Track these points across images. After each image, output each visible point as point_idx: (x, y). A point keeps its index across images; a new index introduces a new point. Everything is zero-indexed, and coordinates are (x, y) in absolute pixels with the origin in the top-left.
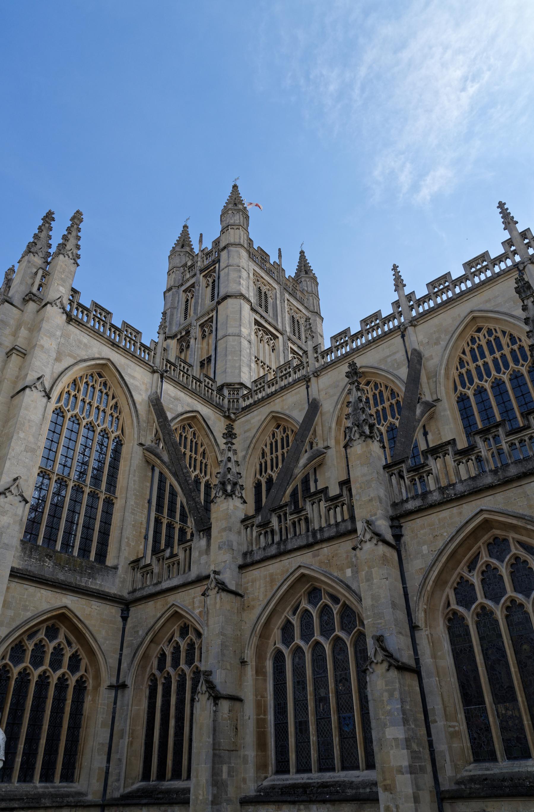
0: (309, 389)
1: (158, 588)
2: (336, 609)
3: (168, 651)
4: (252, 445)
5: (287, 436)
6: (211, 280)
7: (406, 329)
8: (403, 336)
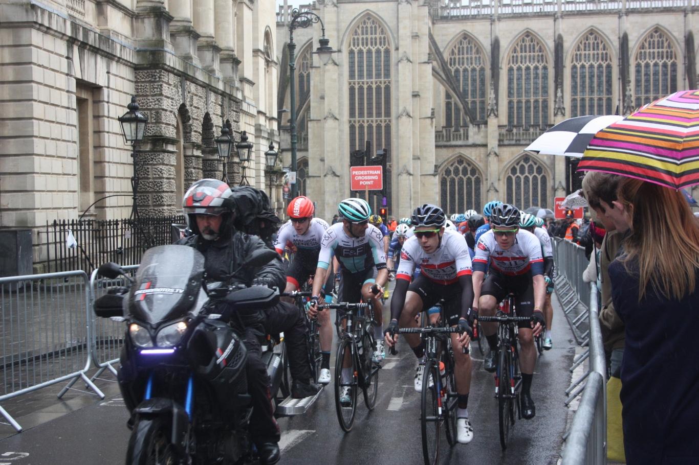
0: (493, 26)
1: (448, 143)
2: (535, 167)
3: (452, 169)
4: (448, 47)
5: (471, 47)
7: (557, 18)
8: (555, 21)
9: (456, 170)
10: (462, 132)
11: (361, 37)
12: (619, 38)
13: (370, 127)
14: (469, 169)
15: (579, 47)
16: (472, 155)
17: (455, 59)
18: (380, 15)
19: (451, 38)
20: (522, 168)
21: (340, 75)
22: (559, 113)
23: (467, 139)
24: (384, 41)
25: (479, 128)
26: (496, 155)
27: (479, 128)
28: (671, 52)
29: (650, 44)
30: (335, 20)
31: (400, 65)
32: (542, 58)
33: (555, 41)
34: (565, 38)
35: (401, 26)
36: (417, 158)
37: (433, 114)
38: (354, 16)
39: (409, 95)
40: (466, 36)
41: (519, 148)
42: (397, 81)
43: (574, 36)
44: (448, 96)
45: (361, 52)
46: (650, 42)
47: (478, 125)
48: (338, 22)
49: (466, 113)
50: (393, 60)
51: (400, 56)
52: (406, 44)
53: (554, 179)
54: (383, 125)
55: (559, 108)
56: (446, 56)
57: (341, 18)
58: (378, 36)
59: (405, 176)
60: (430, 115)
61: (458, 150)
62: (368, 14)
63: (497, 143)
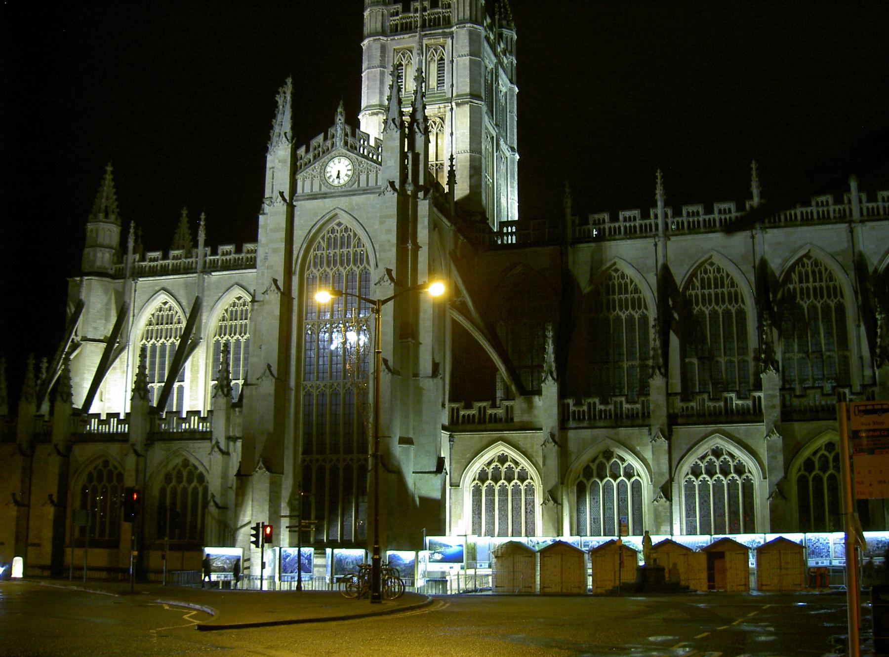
3: (490, 471)
12: (754, 267)
24: (359, 259)
33: (656, 275)
34: (673, 271)
38: (315, 220)
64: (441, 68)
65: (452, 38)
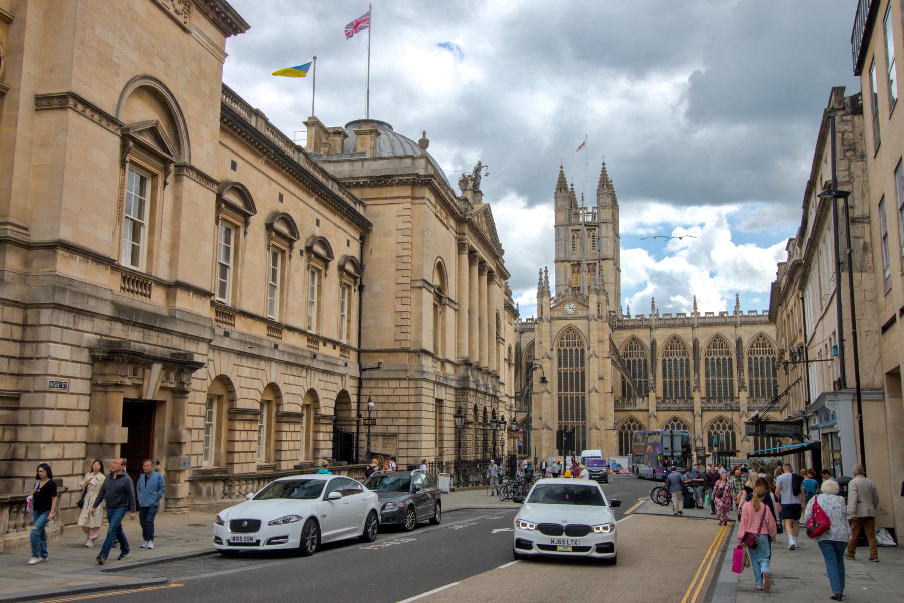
1: (623, 409)
2: (682, 425)
3: (626, 425)
6: (591, 235)
9: (629, 425)
10: (632, 401)
11: (565, 341)
13: (571, 398)
14: (637, 426)
15: (709, 346)
16: (640, 416)
17: (627, 353)
18: (578, 327)
19: (624, 339)
20: (673, 426)
21: (552, 365)
22: (696, 390)
23: (636, 406)
24: (580, 344)
25: (643, 399)
26: (655, 417)
27: (643, 399)
28: (772, 350)
29: (757, 345)
30: (549, 330)
31: (590, 359)
32: (684, 354)
34: (699, 341)
35: (591, 334)
36: (602, 419)
37: (612, 390)
38: (561, 328)
39: (597, 378)
40: (634, 338)
41: (670, 412)
42: (589, 369)
43: (706, 339)
44: (623, 377)
45: (565, 350)
46: (757, 343)
47: (643, 398)
48: (551, 332)
49: (634, 389)
50: (586, 356)
51: (591, 353)
52: (594, 346)
53: (694, 433)
54: (580, 397)
55: (695, 387)
56: (621, 352)
57: (553, 329)
58: (576, 340)
59: (594, 430)
60: (610, 391)
61: (630, 413)
62: (570, 327)
63: (655, 409)
64: (593, 242)
65: (598, 227)
